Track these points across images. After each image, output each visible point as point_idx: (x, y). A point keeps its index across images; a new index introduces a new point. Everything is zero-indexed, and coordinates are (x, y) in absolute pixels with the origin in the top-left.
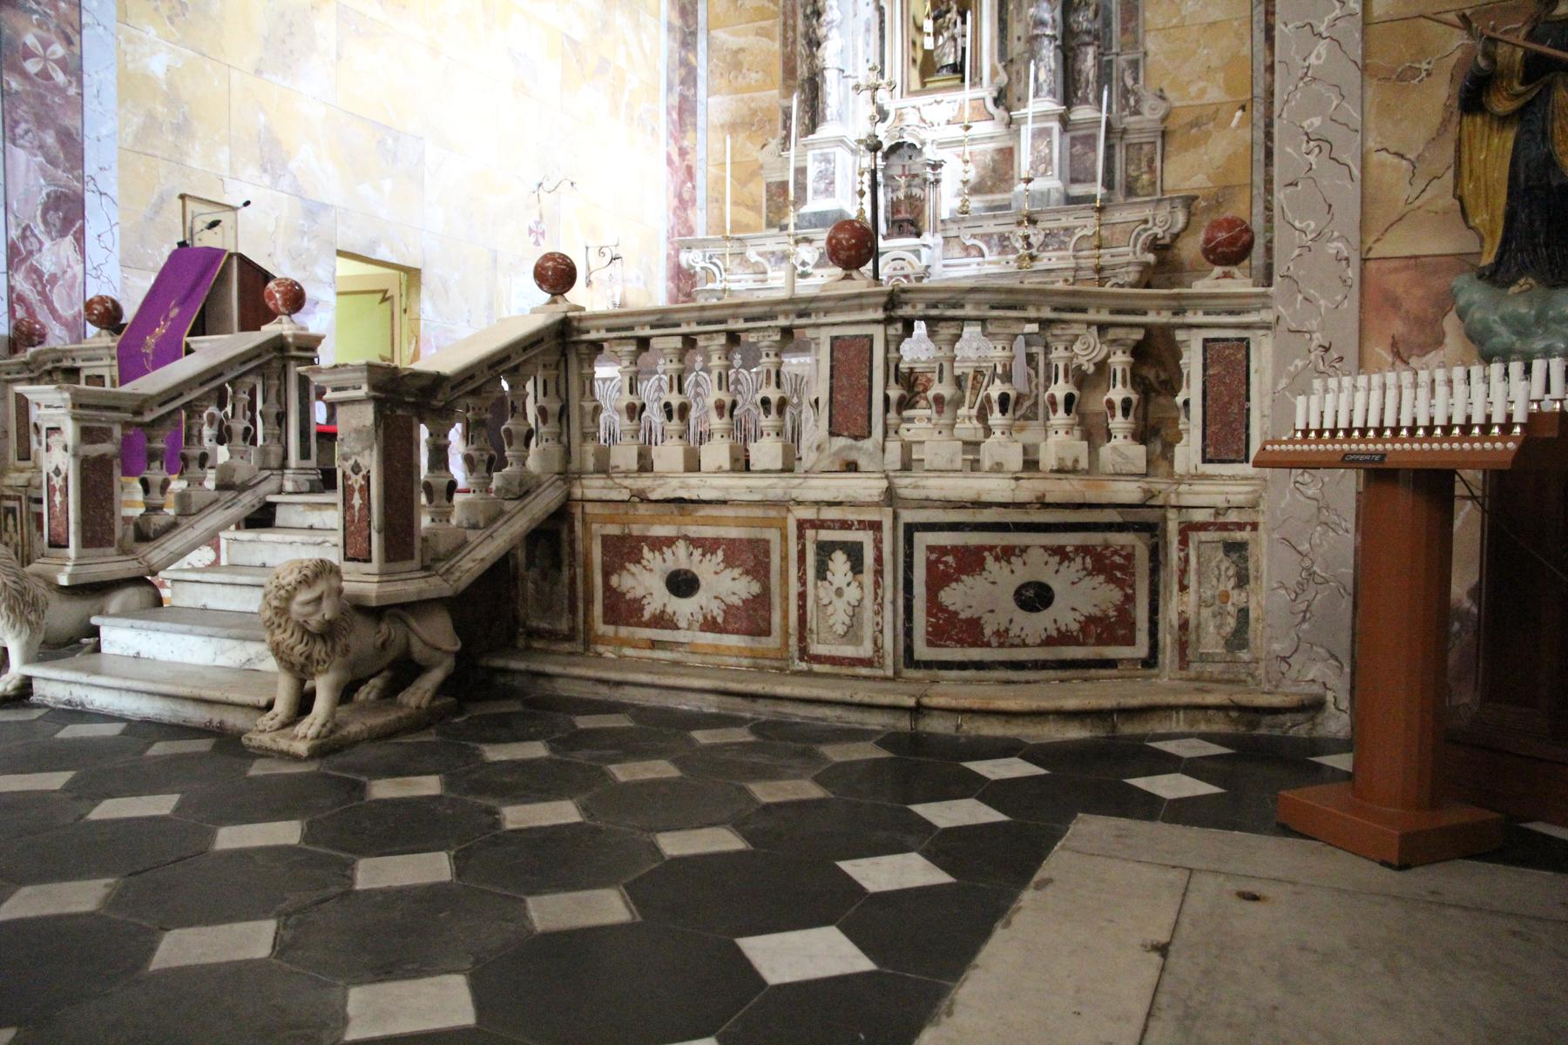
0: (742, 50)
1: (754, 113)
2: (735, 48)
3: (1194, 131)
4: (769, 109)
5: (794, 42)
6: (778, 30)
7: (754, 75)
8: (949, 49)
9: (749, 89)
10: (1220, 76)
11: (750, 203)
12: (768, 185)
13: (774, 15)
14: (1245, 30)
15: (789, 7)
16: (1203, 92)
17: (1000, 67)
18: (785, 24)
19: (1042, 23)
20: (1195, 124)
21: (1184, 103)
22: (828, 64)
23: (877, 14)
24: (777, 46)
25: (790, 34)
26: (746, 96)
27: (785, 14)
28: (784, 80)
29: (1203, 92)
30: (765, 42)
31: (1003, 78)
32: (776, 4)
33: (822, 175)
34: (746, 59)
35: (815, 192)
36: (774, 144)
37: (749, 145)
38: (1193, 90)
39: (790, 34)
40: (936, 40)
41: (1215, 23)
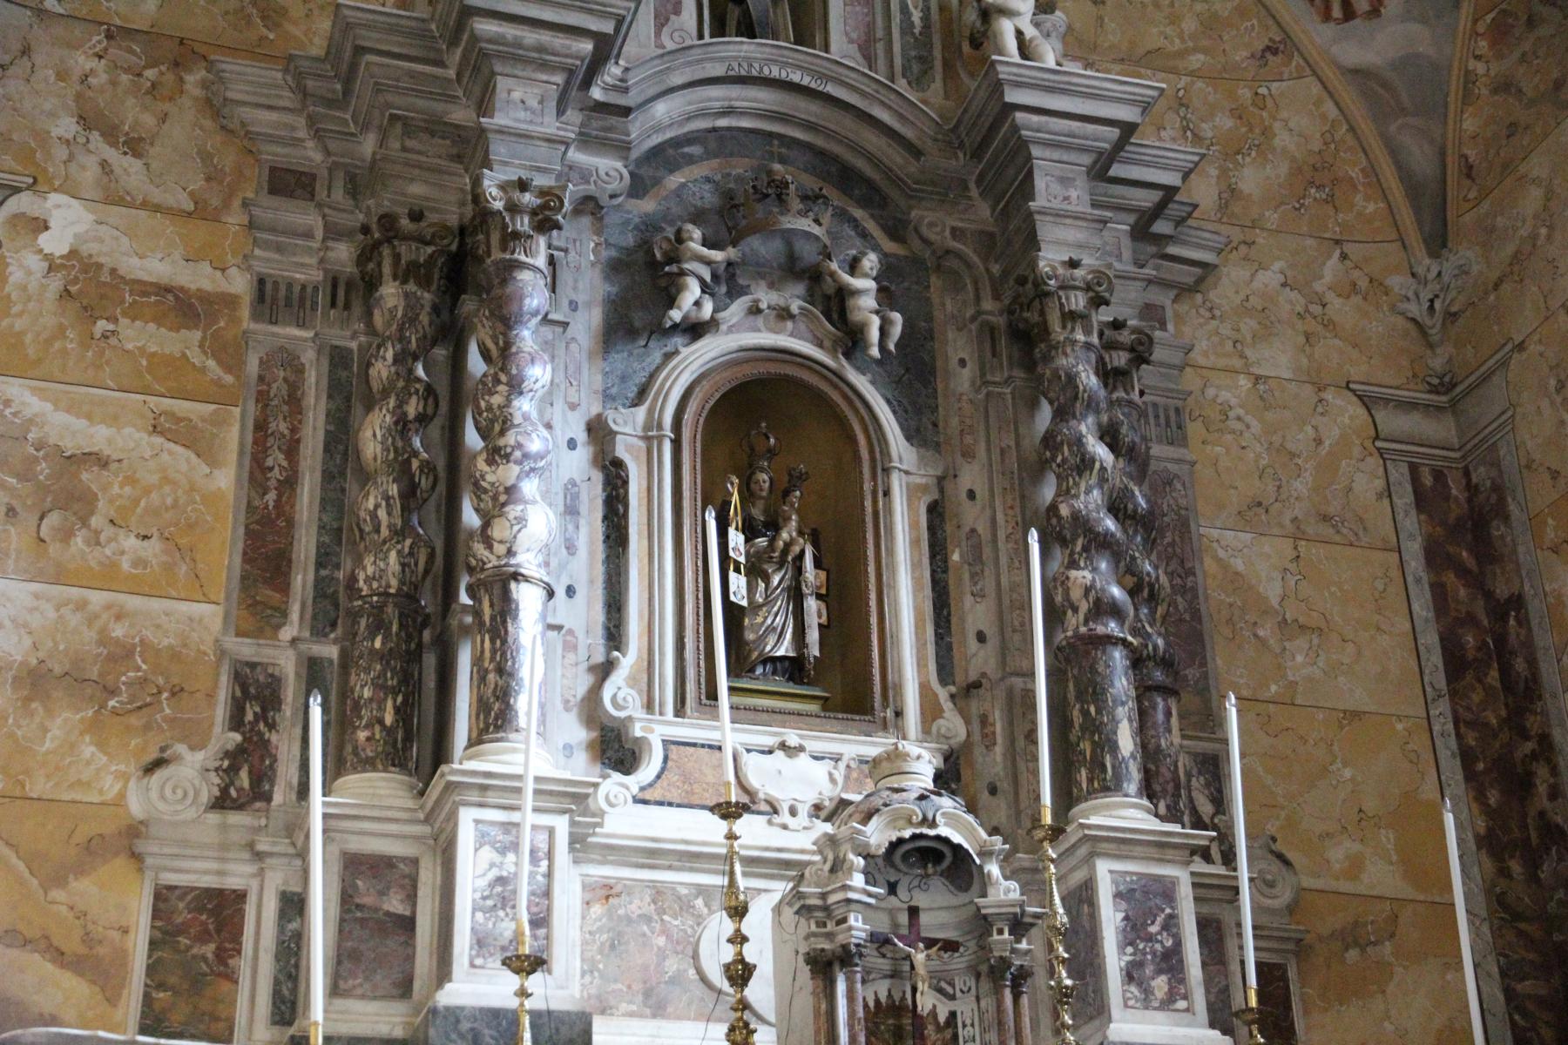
0: (100, 461)
1: (121, 654)
2: (70, 446)
3: (1353, 955)
4: (175, 656)
5: (290, 483)
6: (233, 436)
7: (131, 542)
8: (779, 615)
9: (108, 577)
10: (1387, 838)
11: (73, 945)
12: (162, 896)
13: (222, 397)
14: (1420, 743)
15: (278, 388)
16: (1355, 867)
17: (943, 694)
18: (261, 426)
19: (1115, 611)
20: (1351, 937)
21: (1319, 884)
22: (527, 561)
23: (598, 477)
24: (225, 479)
25: (276, 458)
26: (97, 598)
27: (262, 398)
28: (247, 581)
29: (1355, 867)
30: (180, 458)
31: (954, 725)
32: (233, 364)
33: (501, 893)
34: (110, 491)
35: (481, 942)
36: (194, 769)
37: (88, 750)
38: (1337, 854)
39: (276, 458)
40: (751, 589)
41: (1355, 715)
